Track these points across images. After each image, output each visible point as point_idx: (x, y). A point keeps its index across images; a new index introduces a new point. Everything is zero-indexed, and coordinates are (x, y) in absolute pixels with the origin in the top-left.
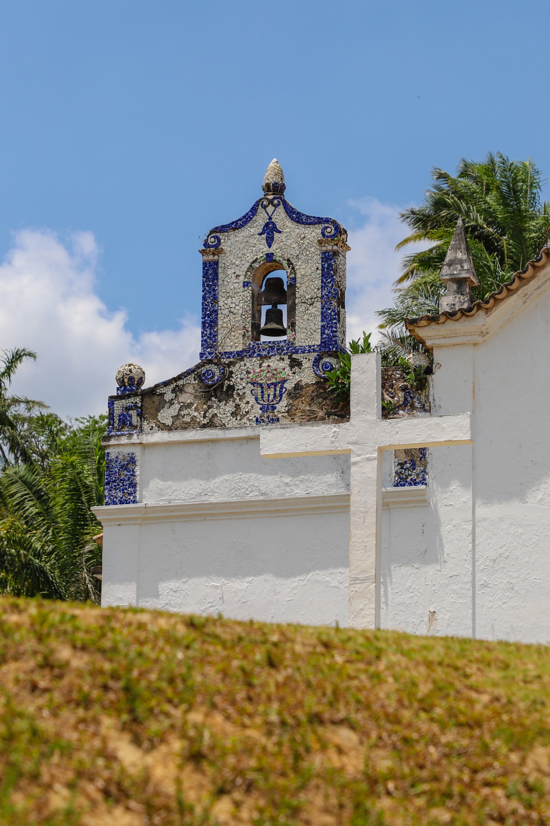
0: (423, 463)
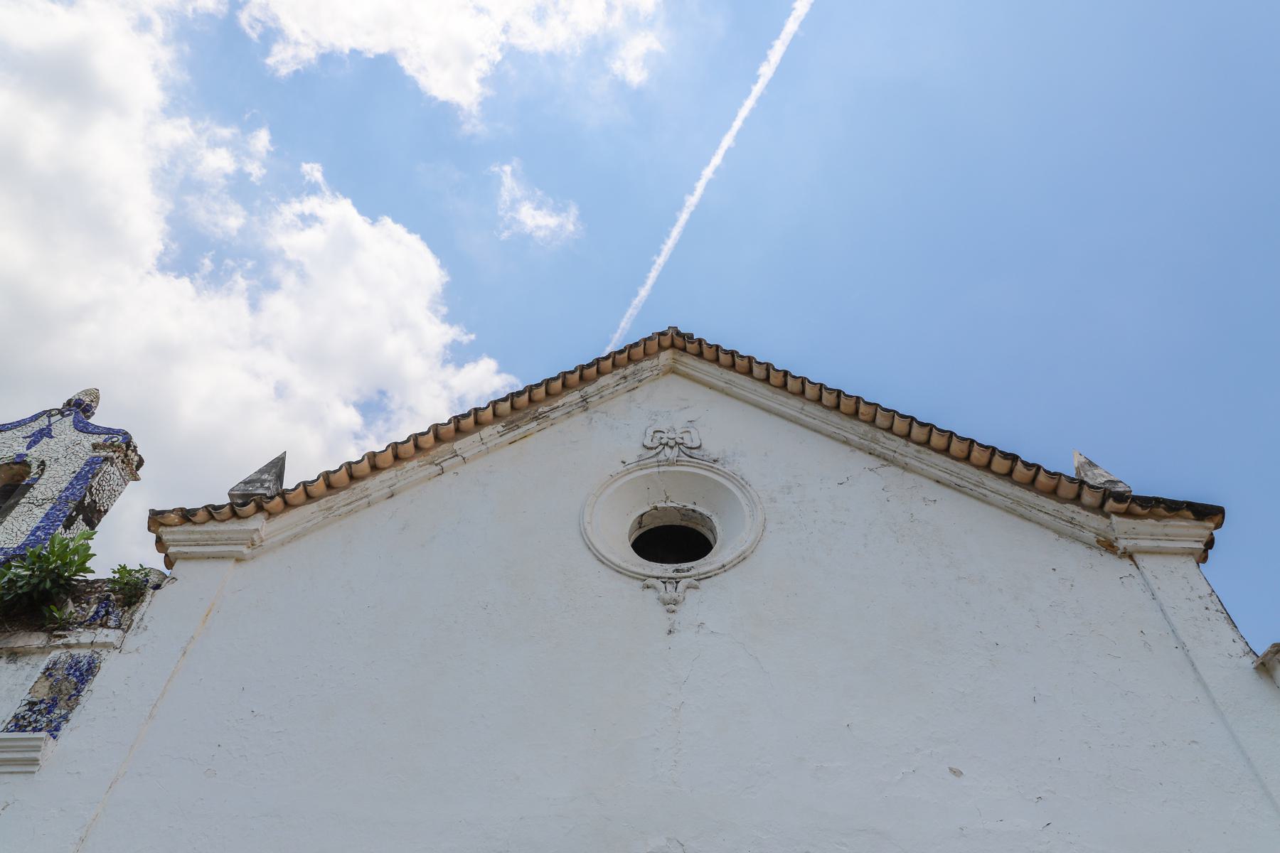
0: (70, 704)
